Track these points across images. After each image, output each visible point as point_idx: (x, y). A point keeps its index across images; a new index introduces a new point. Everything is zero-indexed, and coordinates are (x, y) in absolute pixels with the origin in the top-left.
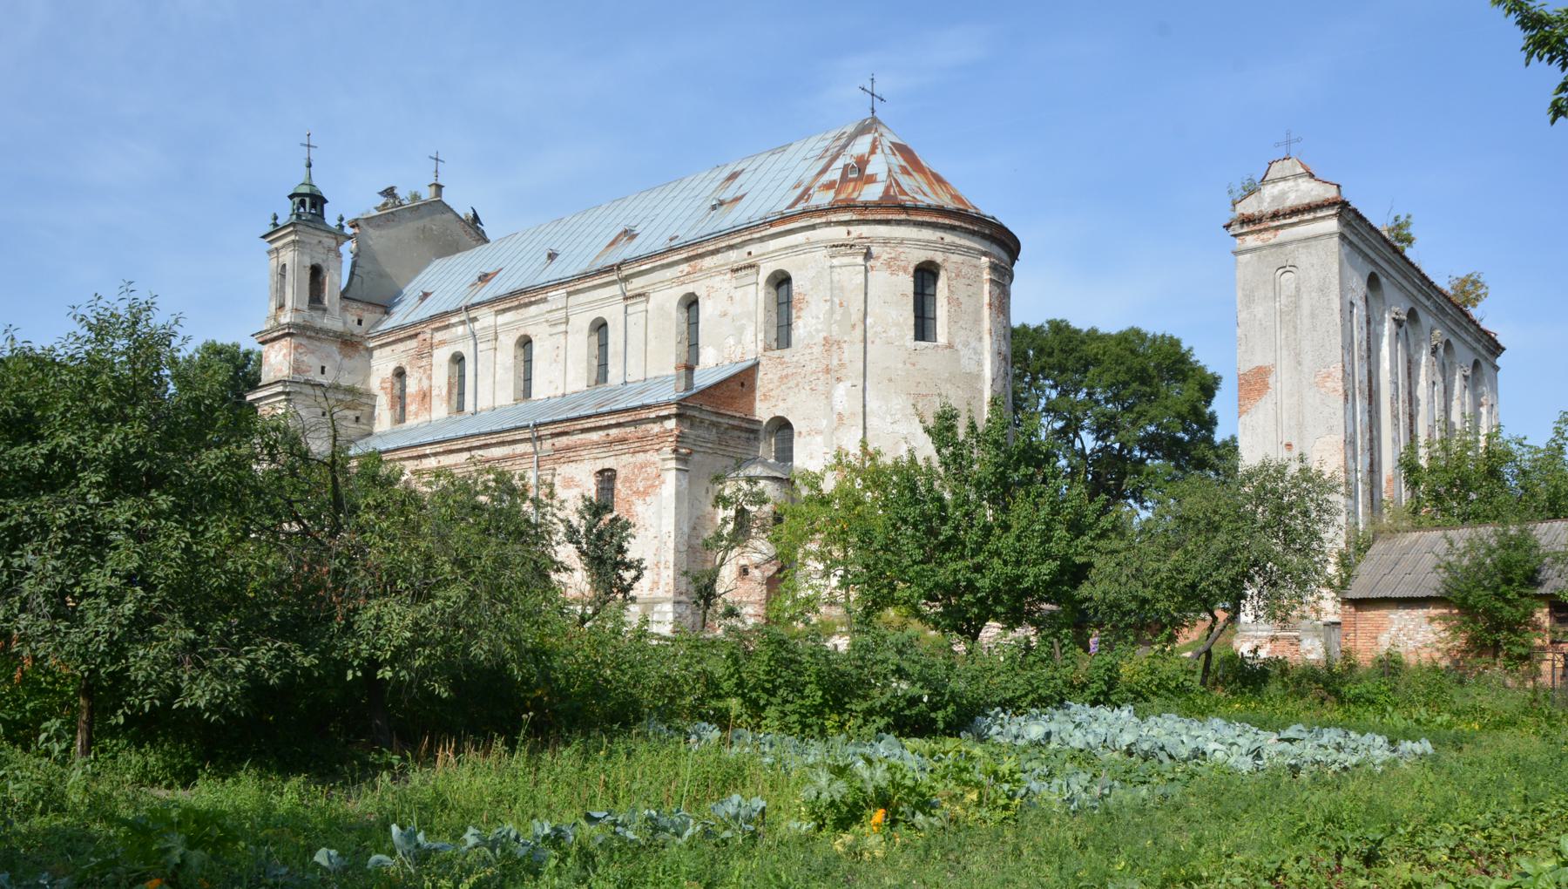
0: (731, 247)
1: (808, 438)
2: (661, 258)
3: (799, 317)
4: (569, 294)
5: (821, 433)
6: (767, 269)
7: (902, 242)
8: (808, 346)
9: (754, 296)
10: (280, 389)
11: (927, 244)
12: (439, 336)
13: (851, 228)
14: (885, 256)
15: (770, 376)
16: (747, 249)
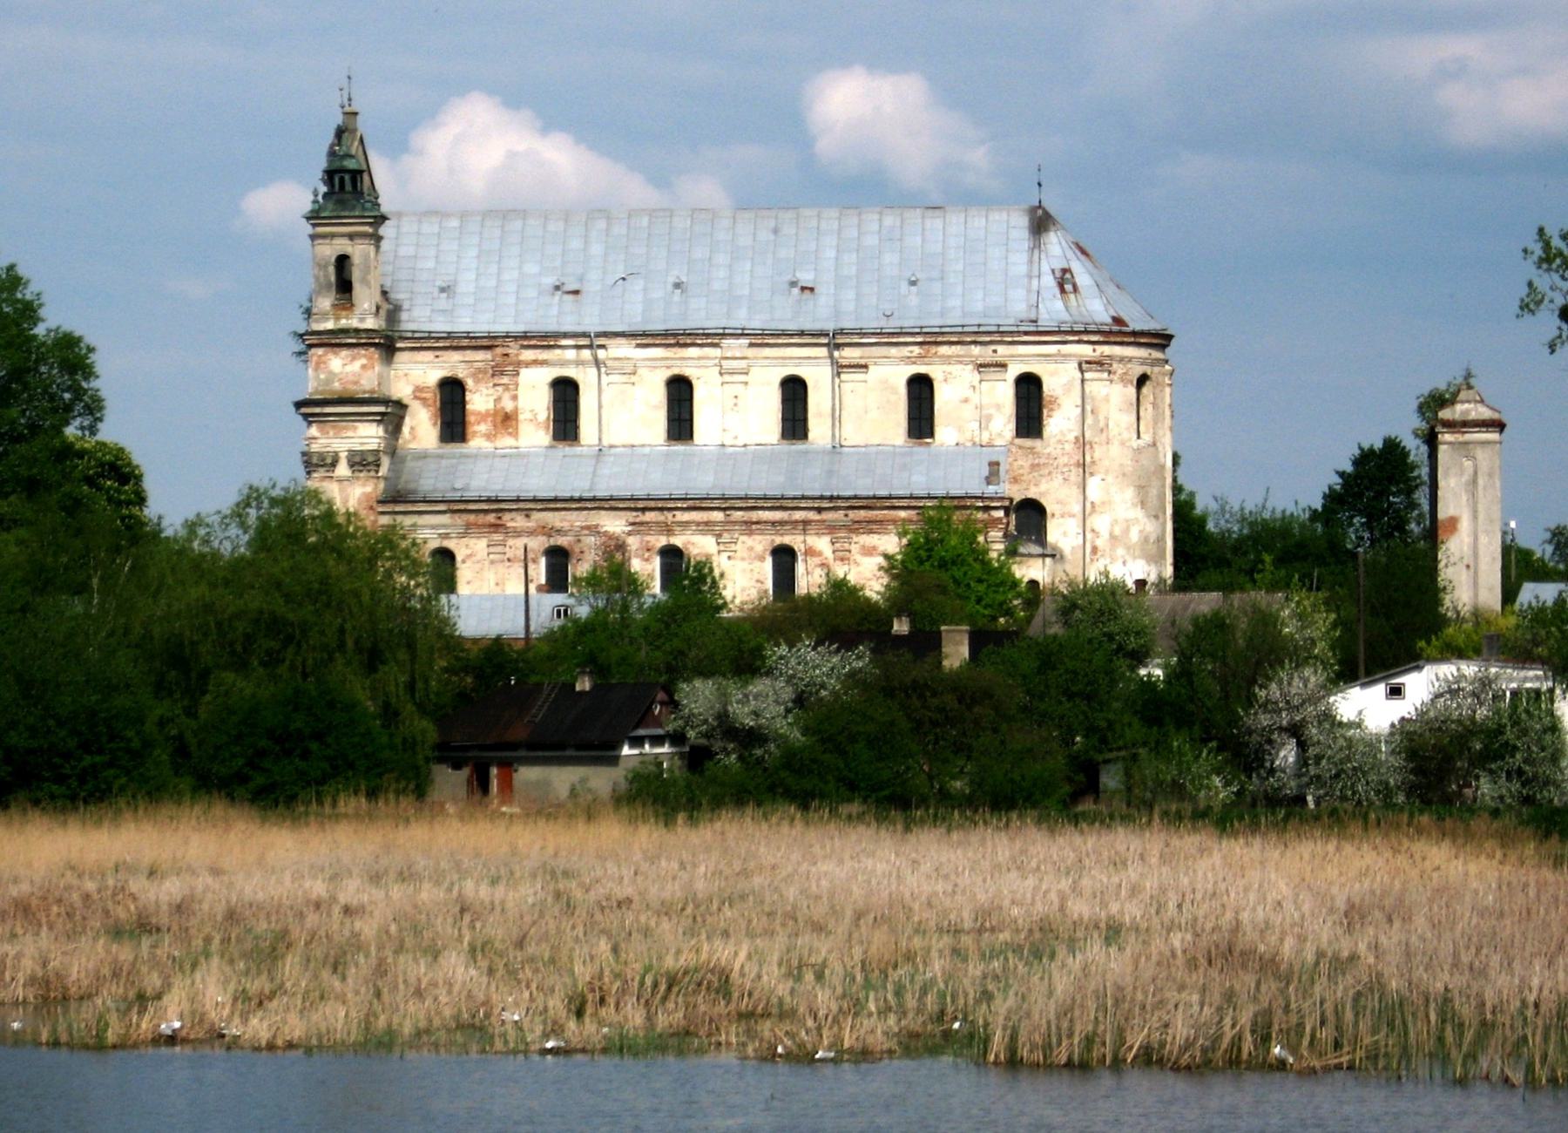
0: (975, 343)
1: (1061, 520)
2: (890, 337)
3: (1049, 416)
4: (751, 345)
5: (1074, 516)
6: (1015, 370)
7: (1130, 360)
8: (1060, 442)
9: (1003, 394)
10: (382, 409)
11: (1143, 362)
12: (528, 355)
13: (1097, 347)
14: (1120, 371)
15: (1020, 462)
16: (993, 347)
